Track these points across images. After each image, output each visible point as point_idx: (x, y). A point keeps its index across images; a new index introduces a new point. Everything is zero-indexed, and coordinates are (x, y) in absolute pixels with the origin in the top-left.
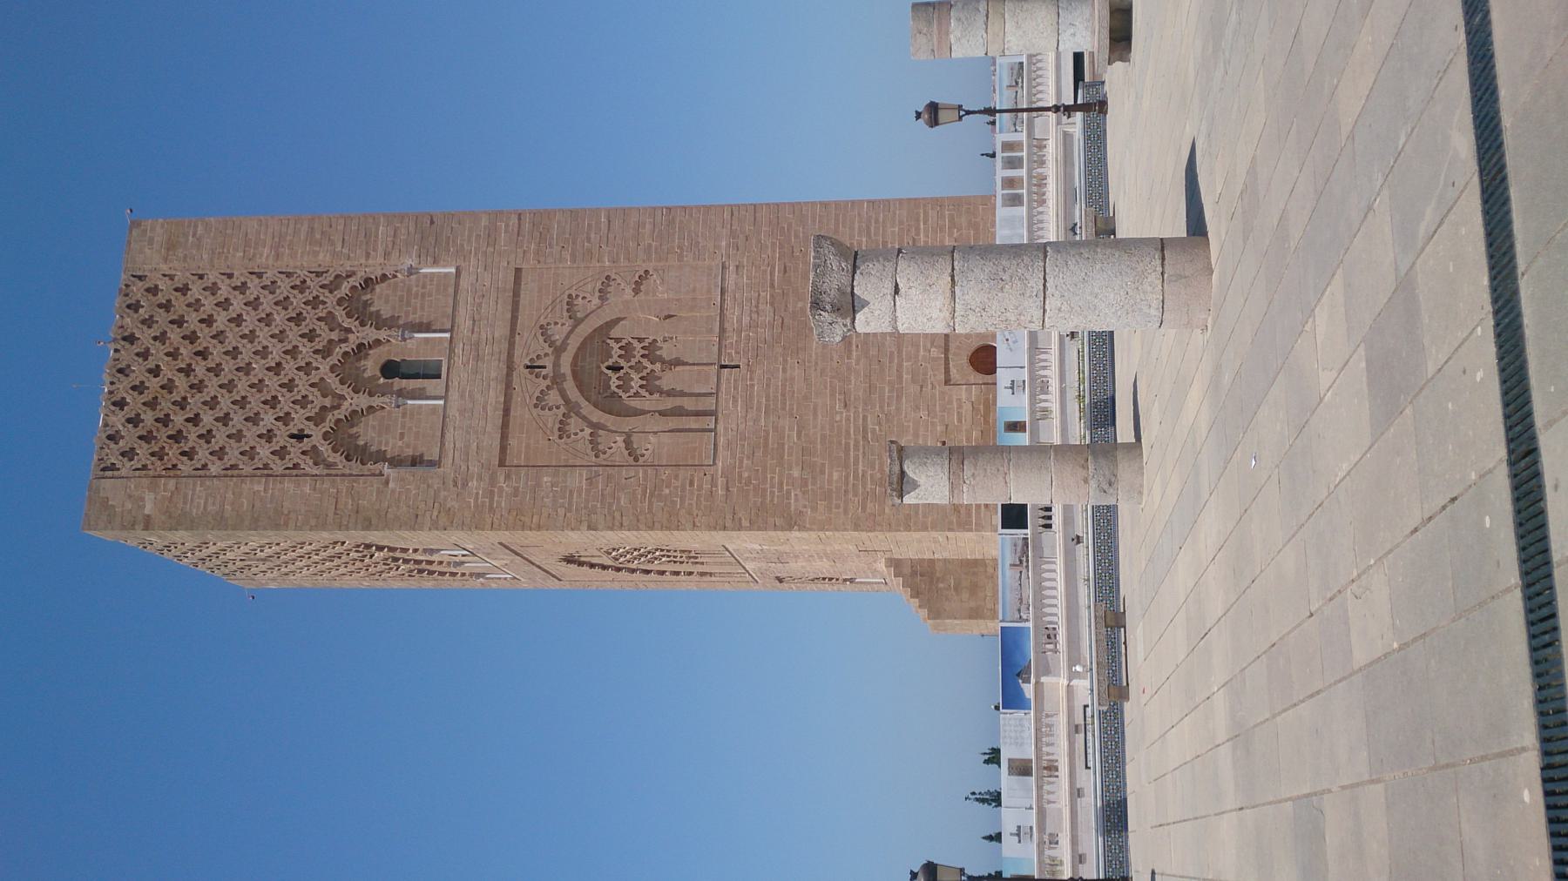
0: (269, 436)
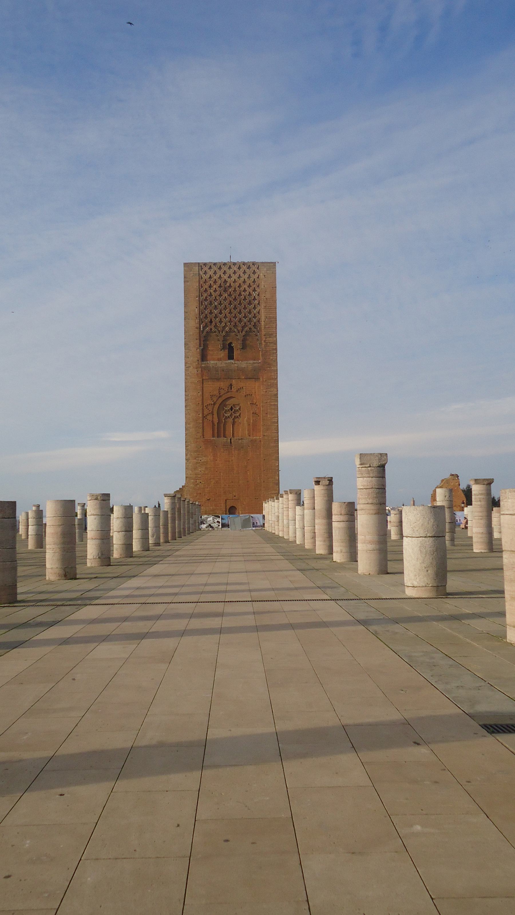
0: (211, 313)
